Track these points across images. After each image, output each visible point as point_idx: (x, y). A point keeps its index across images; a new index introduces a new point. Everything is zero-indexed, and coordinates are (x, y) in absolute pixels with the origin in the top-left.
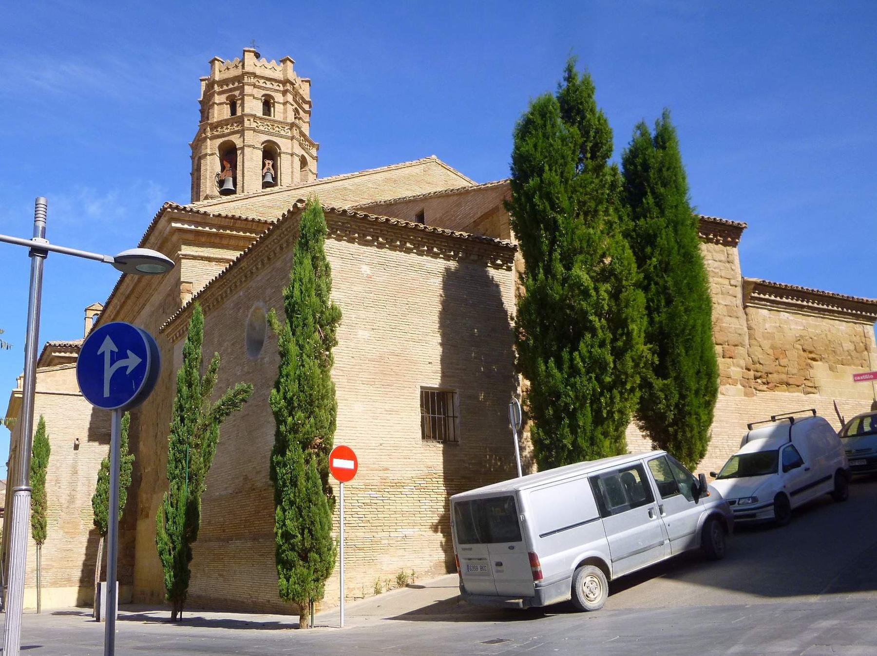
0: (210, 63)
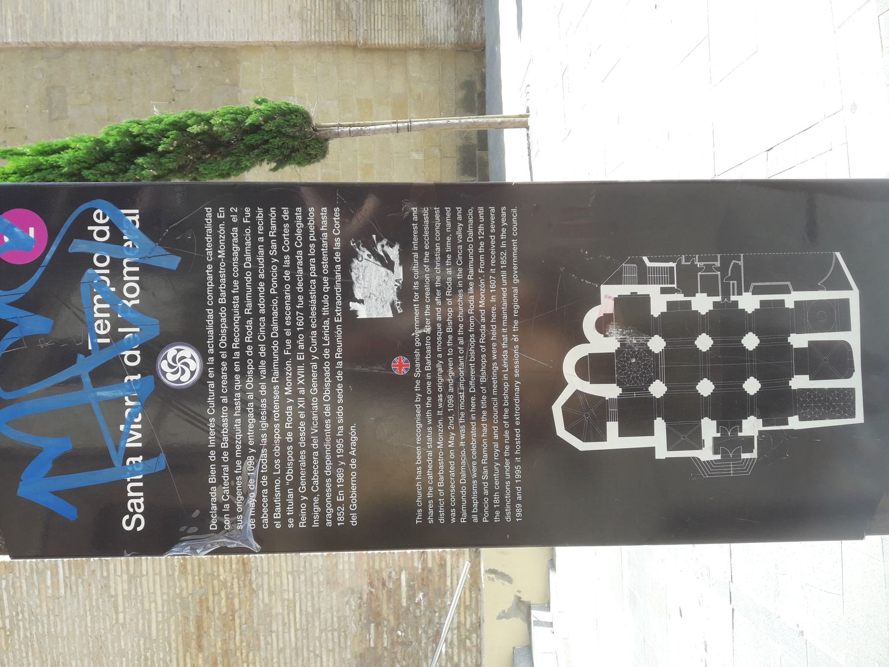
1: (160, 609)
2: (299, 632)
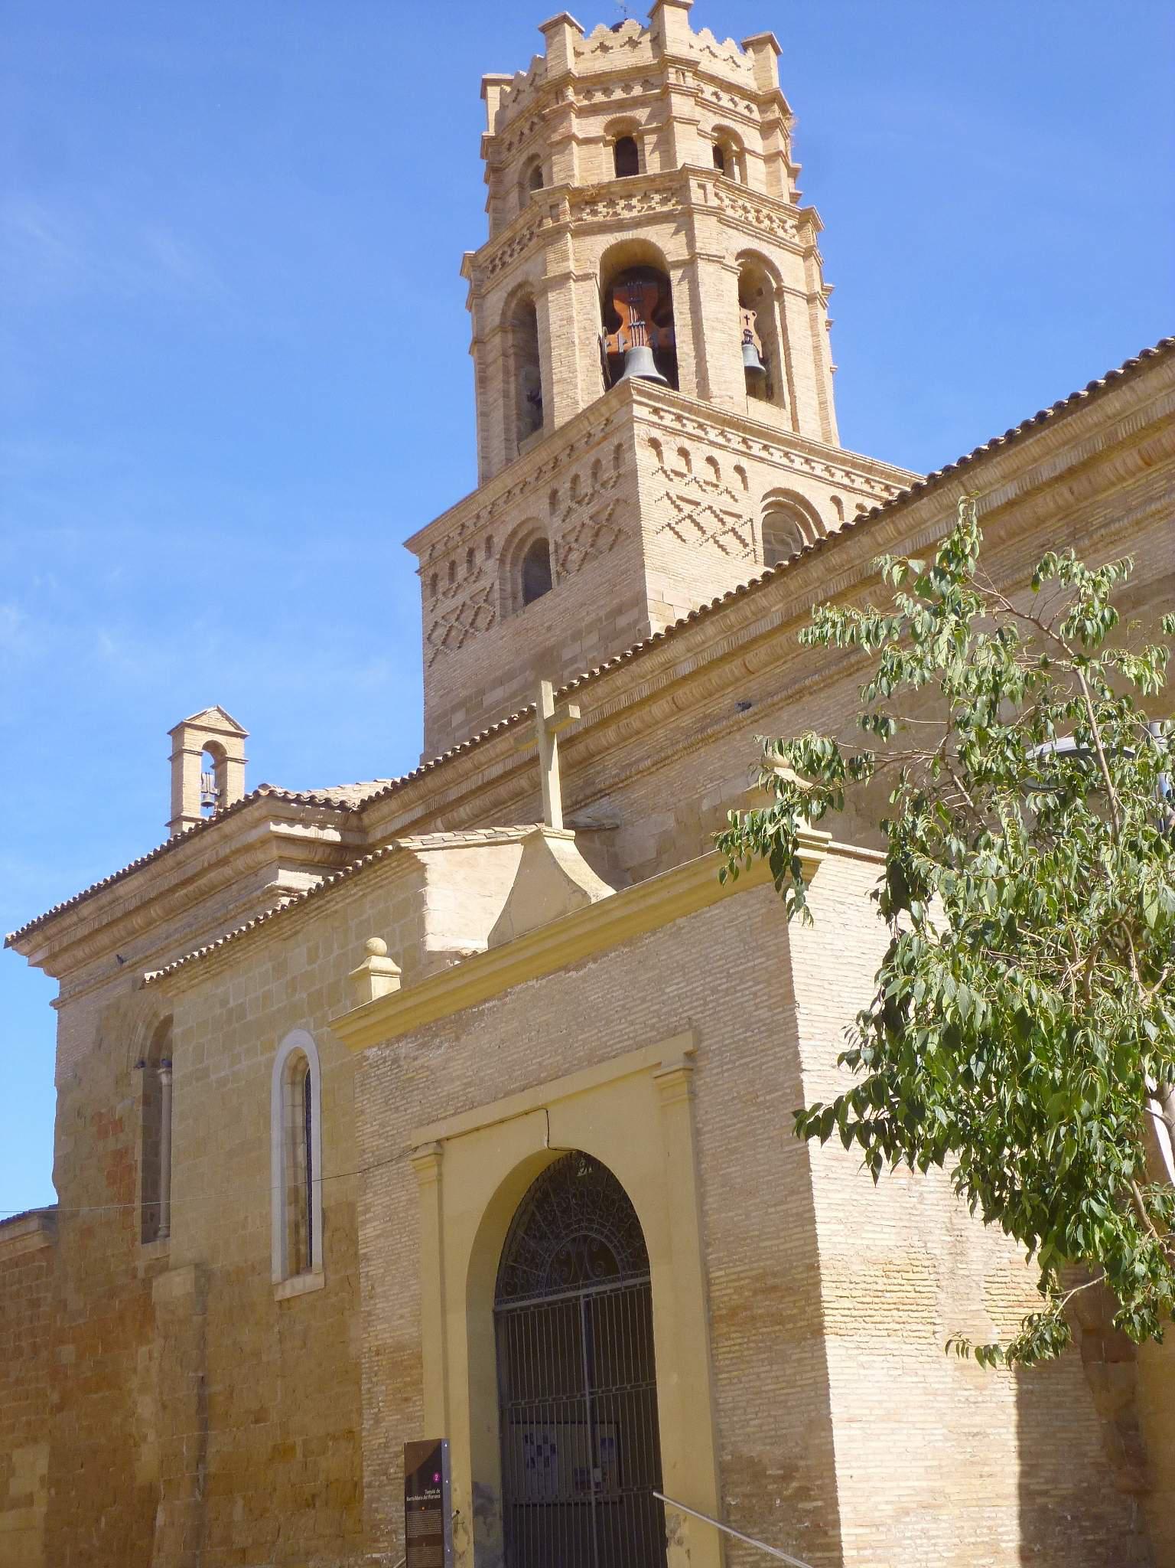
0: (543, 30)
1: (781, 1247)
2: (772, 1394)
